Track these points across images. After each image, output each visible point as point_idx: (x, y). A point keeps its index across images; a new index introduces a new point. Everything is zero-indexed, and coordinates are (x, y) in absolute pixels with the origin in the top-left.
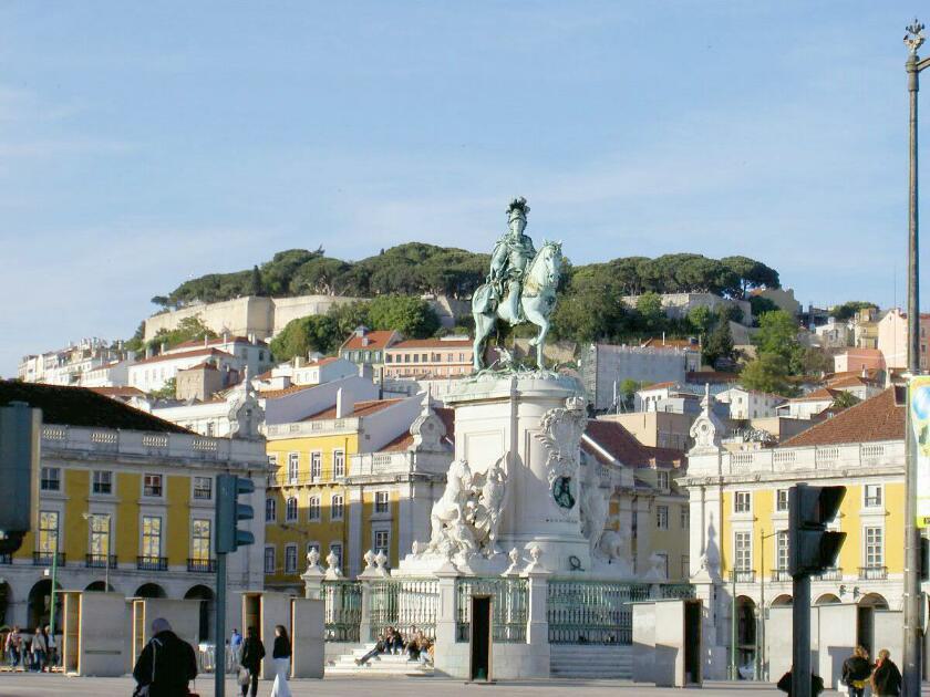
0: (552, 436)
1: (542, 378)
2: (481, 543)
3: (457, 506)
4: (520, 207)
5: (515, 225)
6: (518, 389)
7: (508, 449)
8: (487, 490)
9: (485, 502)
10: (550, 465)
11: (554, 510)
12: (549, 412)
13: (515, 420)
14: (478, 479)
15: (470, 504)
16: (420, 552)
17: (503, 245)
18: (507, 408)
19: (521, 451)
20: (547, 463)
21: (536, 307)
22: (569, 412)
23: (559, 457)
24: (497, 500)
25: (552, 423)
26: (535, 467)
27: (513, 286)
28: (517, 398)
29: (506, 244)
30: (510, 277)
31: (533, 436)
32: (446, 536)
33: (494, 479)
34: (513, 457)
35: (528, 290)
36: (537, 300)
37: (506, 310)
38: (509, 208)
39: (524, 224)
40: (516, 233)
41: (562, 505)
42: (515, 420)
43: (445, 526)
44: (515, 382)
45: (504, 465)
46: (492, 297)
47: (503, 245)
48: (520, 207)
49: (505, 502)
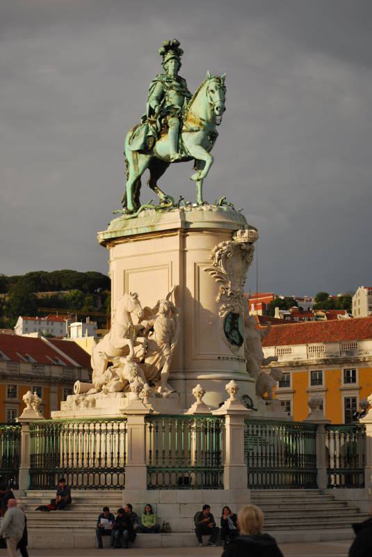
1: (211, 210)
2: (151, 377)
3: (128, 342)
4: (174, 48)
5: (171, 66)
6: (188, 219)
7: (177, 282)
8: (159, 323)
10: (221, 301)
11: (224, 348)
12: (220, 245)
13: (183, 252)
14: (148, 314)
15: (141, 339)
16: (83, 392)
17: (159, 84)
18: (175, 240)
19: (190, 285)
20: (218, 298)
21: (199, 142)
22: (240, 245)
23: (229, 293)
24: (169, 336)
25: (224, 257)
26: (205, 302)
27: (172, 122)
28: (185, 230)
29: (163, 82)
30: (168, 113)
31: (202, 269)
32: (114, 375)
33: (166, 313)
34: (180, 292)
35: (189, 125)
36: (200, 134)
37: (164, 147)
38: (162, 49)
39: (178, 66)
40: (171, 72)
41: (233, 343)
42: (183, 252)
43: (110, 364)
44: (183, 213)
45: (172, 299)
46: (150, 133)
47: (159, 84)
48: (174, 48)
49: (176, 338)
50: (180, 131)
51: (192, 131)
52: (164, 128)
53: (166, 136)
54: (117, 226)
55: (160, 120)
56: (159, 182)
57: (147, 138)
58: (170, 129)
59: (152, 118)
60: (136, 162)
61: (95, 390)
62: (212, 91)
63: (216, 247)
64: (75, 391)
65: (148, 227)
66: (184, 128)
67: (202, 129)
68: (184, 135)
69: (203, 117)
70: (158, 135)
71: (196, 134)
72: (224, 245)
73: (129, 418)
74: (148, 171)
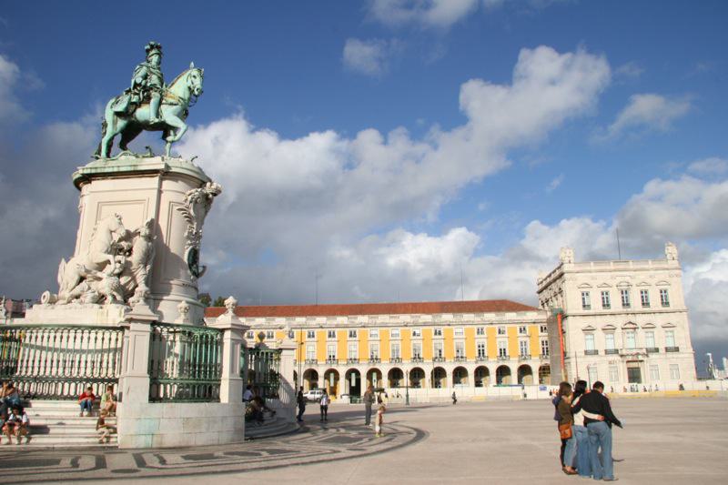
0: (192, 212)
8: (139, 245)
9: (136, 257)
10: (188, 238)
12: (193, 190)
13: (160, 192)
14: (129, 236)
19: (163, 223)
20: (186, 234)
24: (146, 259)
27: (155, 96)
29: (148, 67)
30: (152, 89)
34: (153, 225)
36: (177, 108)
42: (160, 192)
50: (160, 103)
51: (171, 104)
52: (147, 99)
53: (147, 106)
54: (100, 165)
55: (143, 93)
56: (128, 145)
57: (131, 103)
58: (152, 101)
59: (136, 91)
60: (115, 123)
61: (65, 301)
62: (194, 77)
63: (189, 192)
64: (43, 301)
65: (131, 166)
66: (164, 101)
69: (182, 96)
70: (138, 105)
71: (175, 107)
72: (196, 192)
73: (132, 326)
74: (120, 135)
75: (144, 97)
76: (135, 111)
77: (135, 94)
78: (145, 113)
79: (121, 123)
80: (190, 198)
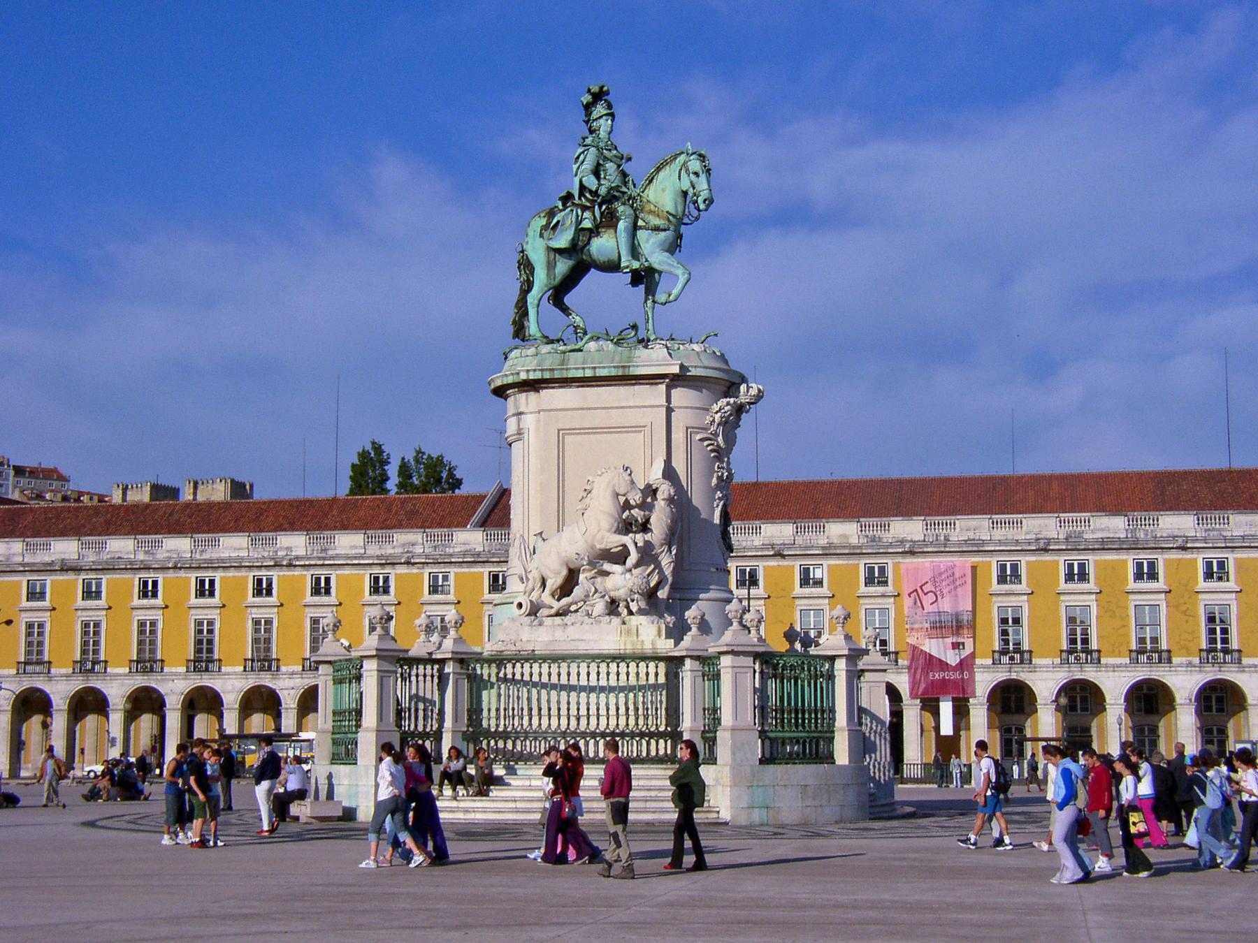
10: (718, 487)
13: (669, 410)
20: (714, 481)
21: (667, 246)
24: (672, 537)
50: (635, 227)
51: (657, 229)
57: (579, 231)
60: (551, 266)
62: (696, 174)
66: (640, 223)
67: (672, 228)
68: (641, 234)
71: (663, 234)
75: (602, 214)
76: (588, 243)
77: (584, 208)
78: (603, 245)
79: (563, 266)
80: (717, 417)
